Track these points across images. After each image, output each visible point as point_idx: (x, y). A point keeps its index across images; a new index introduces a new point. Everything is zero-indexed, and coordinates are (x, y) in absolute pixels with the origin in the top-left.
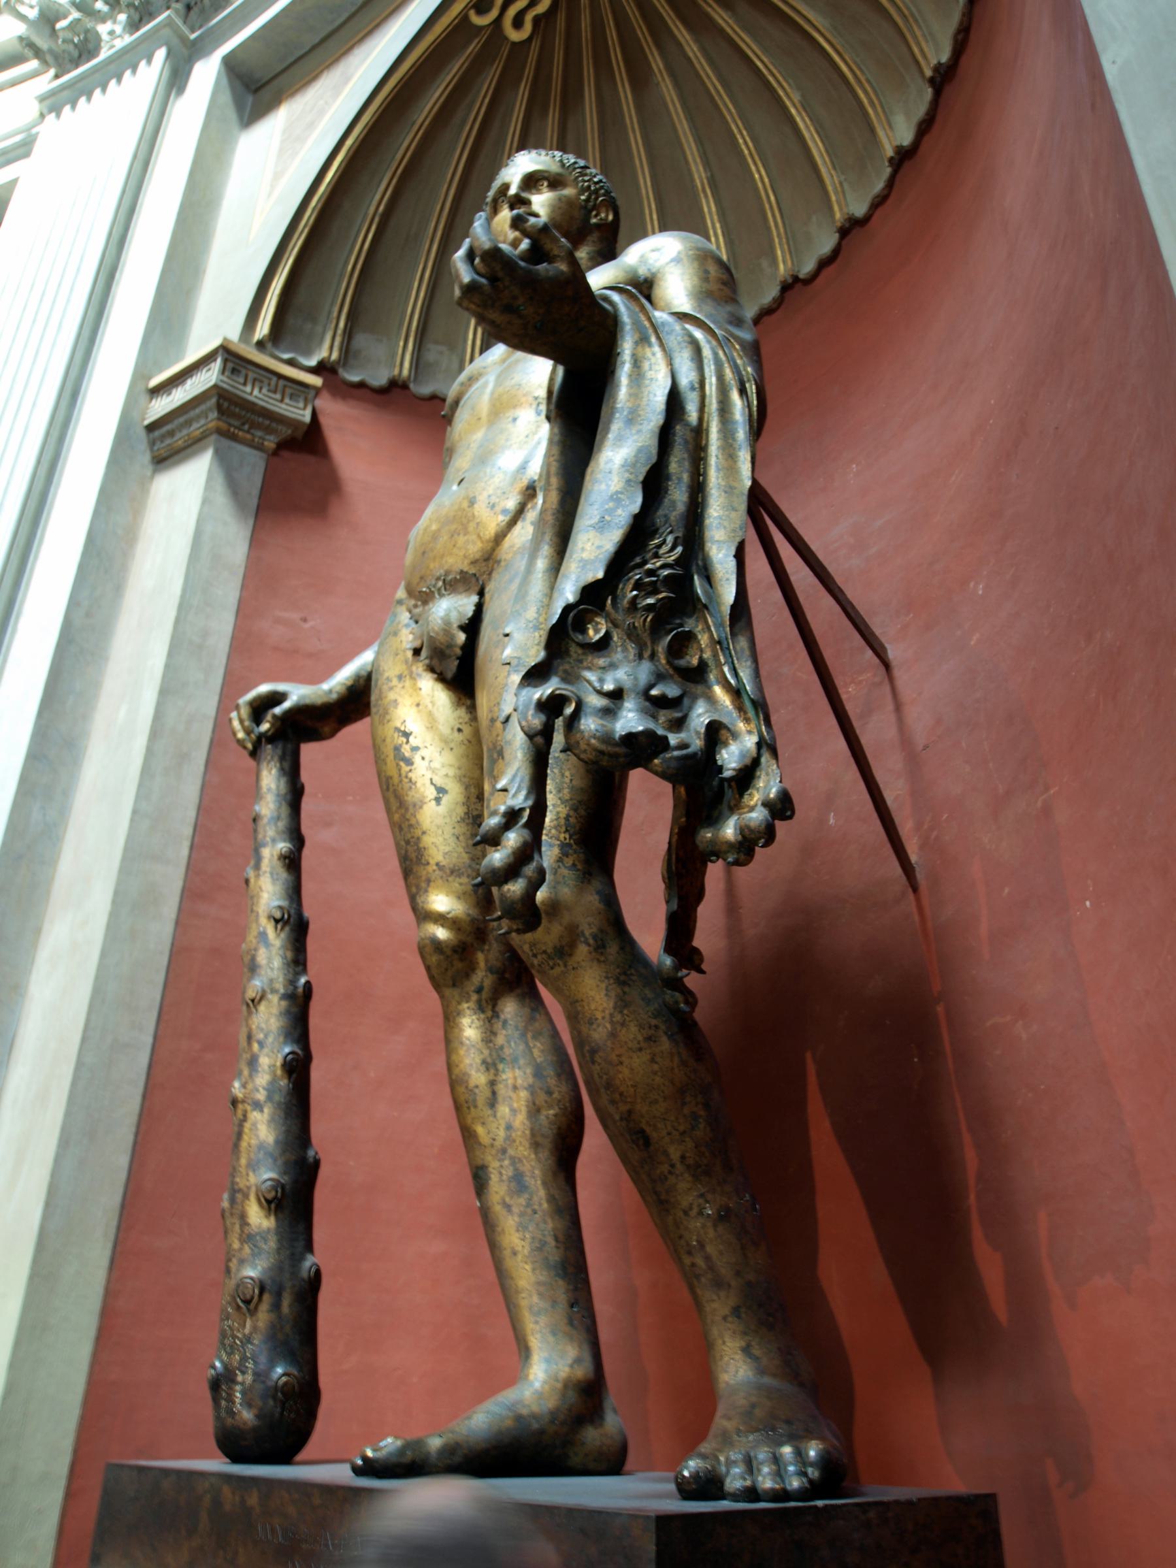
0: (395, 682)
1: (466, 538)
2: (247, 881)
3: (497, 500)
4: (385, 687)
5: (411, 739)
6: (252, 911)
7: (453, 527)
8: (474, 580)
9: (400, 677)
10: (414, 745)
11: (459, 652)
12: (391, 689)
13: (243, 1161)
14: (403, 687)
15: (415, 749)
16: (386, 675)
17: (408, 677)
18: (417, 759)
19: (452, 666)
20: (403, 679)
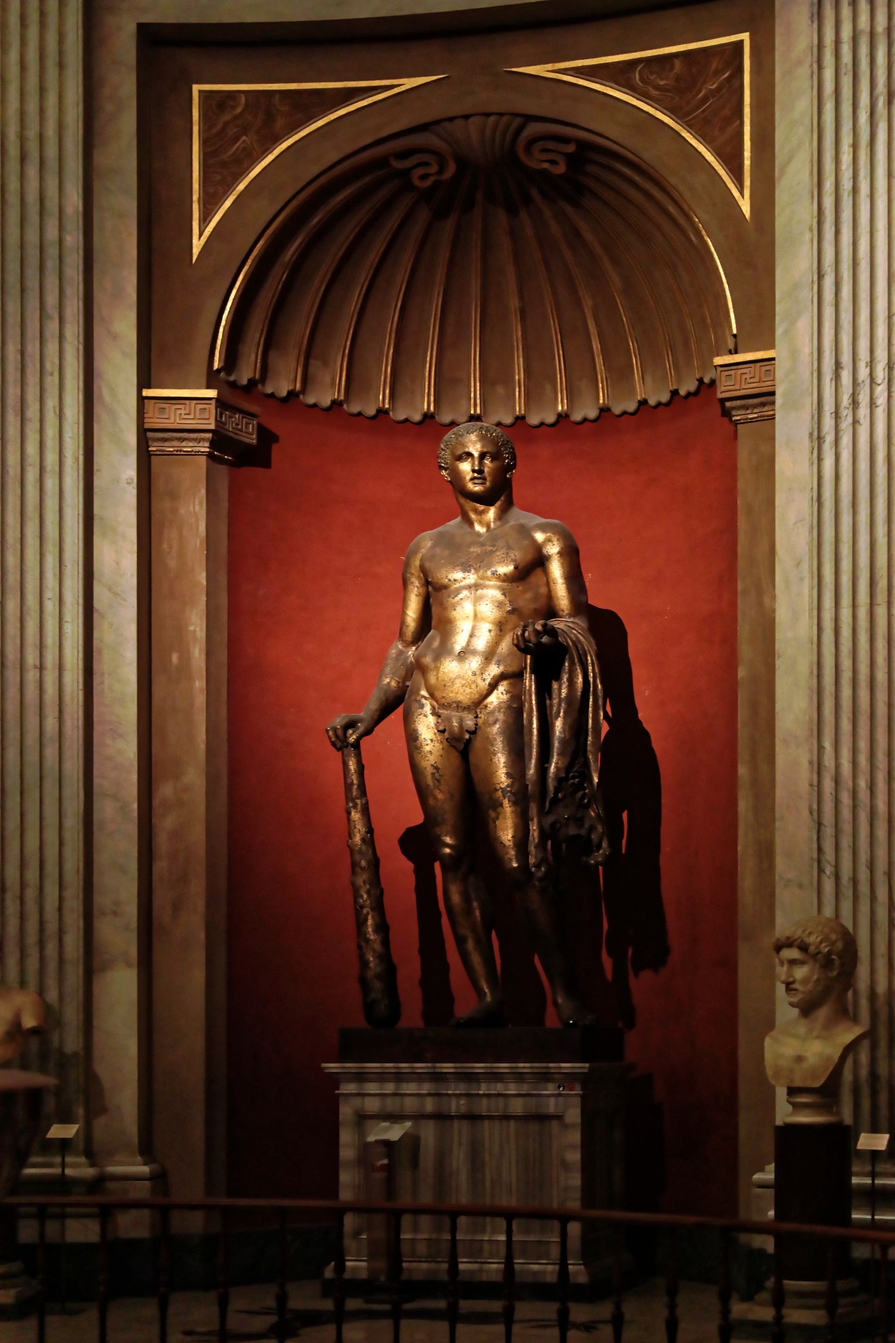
0: (429, 742)
1: (470, 690)
2: (349, 813)
3: (486, 677)
4: (424, 743)
5: (440, 771)
6: (355, 828)
7: (463, 682)
8: (474, 711)
9: (432, 740)
10: (441, 774)
11: (465, 741)
12: (427, 745)
13: (370, 930)
14: (434, 746)
15: (441, 776)
16: (423, 737)
17: (436, 742)
18: (442, 781)
19: (462, 746)
20: (434, 742)
